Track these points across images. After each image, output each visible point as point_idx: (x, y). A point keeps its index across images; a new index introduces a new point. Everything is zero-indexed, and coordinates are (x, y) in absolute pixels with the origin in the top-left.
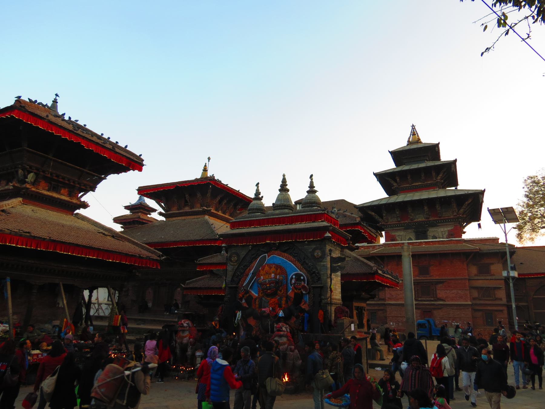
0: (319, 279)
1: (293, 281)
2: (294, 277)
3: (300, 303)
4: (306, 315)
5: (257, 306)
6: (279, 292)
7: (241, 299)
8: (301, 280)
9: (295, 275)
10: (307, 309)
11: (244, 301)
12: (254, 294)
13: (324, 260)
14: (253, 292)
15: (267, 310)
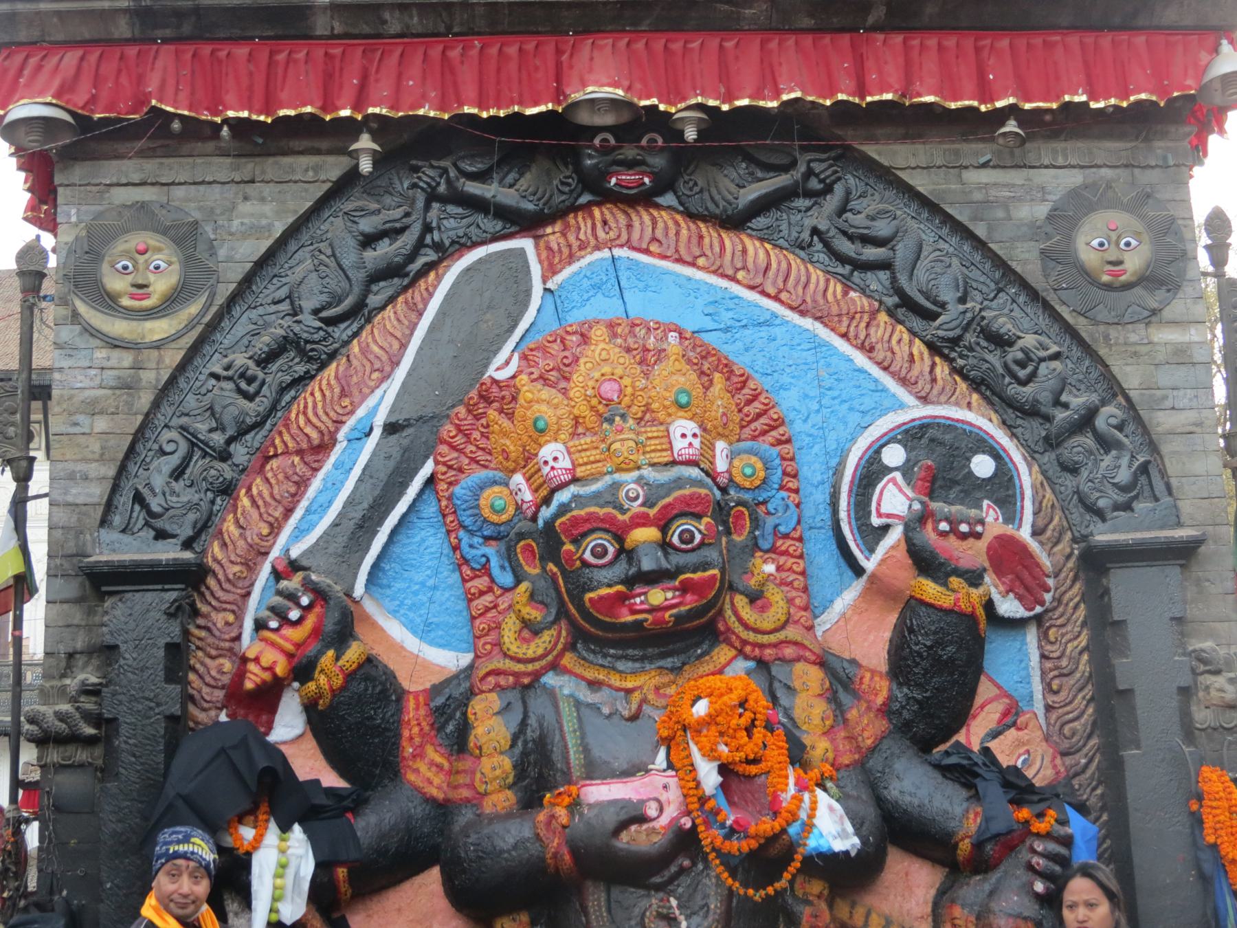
0: (1148, 477)
1: (894, 499)
2: (894, 455)
3: (961, 715)
4: (1078, 826)
5: (495, 765)
6: (741, 601)
7: (265, 700)
8: (973, 489)
9: (912, 435)
10: (1040, 772)
11: (288, 726)
12: (412, 643)
13: (1176, 308)
14: (395, 630)
15: (647, 793)
